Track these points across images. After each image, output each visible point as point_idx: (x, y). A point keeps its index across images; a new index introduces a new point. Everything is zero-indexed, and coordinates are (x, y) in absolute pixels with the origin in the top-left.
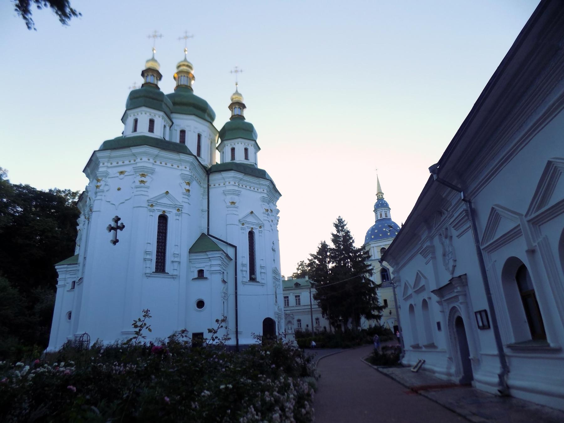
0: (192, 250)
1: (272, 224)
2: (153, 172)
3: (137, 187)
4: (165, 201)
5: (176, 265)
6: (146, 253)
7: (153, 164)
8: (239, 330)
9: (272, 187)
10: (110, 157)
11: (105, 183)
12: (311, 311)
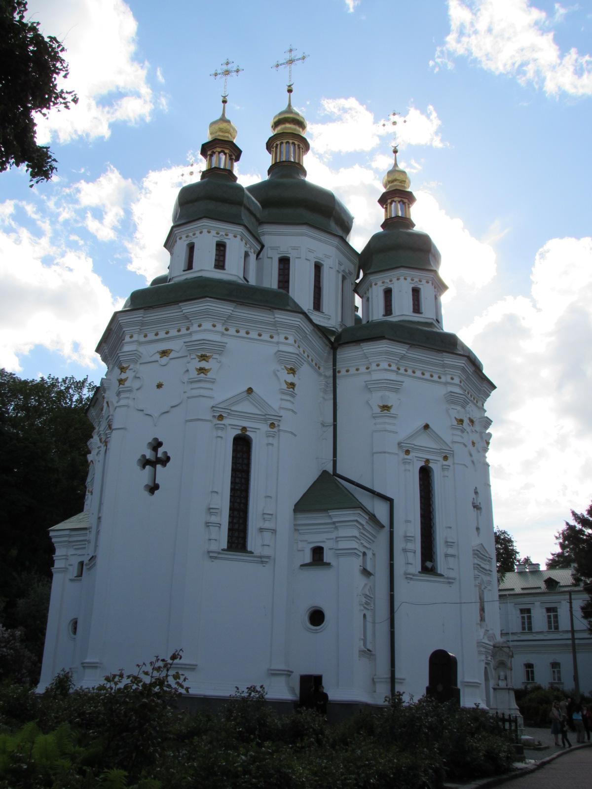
0: (301, 507)
1: (473, 451)
2: (221, 349)
3: (191, 382)
4: (246, 407)
5: (267, 535)
6: (210, 510)
7: (223, 334)
8: (397, 675)
9: (470, 369)
10: (143, 324)
11: (133, 374)
12: (574, 645)
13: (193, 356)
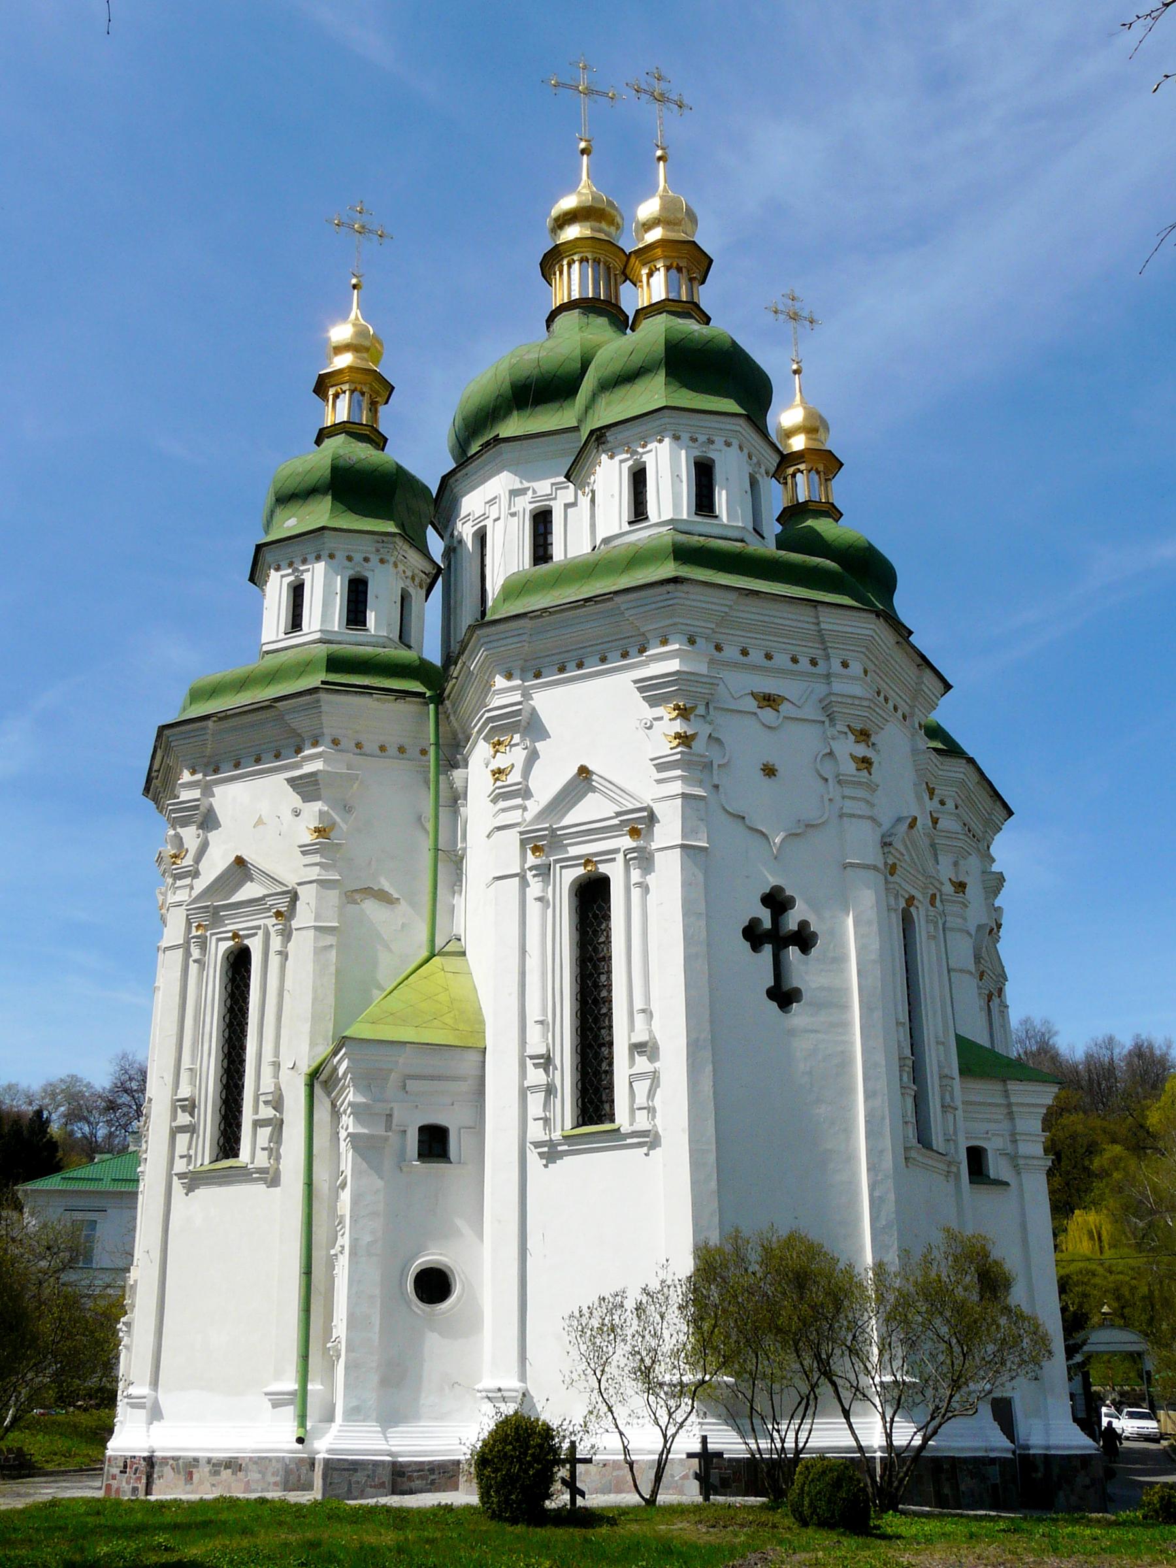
13: (841, 727)
